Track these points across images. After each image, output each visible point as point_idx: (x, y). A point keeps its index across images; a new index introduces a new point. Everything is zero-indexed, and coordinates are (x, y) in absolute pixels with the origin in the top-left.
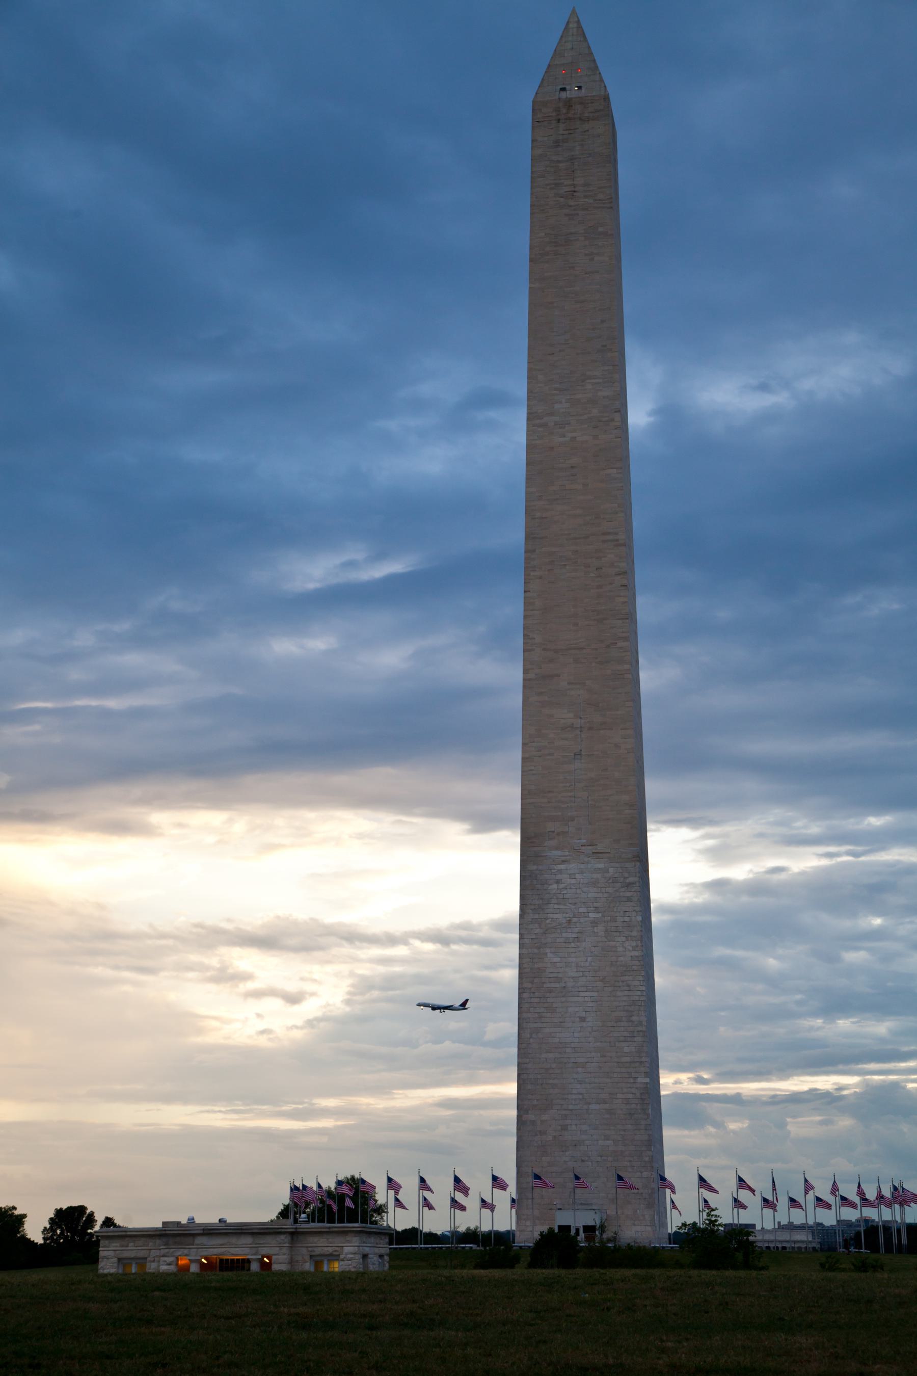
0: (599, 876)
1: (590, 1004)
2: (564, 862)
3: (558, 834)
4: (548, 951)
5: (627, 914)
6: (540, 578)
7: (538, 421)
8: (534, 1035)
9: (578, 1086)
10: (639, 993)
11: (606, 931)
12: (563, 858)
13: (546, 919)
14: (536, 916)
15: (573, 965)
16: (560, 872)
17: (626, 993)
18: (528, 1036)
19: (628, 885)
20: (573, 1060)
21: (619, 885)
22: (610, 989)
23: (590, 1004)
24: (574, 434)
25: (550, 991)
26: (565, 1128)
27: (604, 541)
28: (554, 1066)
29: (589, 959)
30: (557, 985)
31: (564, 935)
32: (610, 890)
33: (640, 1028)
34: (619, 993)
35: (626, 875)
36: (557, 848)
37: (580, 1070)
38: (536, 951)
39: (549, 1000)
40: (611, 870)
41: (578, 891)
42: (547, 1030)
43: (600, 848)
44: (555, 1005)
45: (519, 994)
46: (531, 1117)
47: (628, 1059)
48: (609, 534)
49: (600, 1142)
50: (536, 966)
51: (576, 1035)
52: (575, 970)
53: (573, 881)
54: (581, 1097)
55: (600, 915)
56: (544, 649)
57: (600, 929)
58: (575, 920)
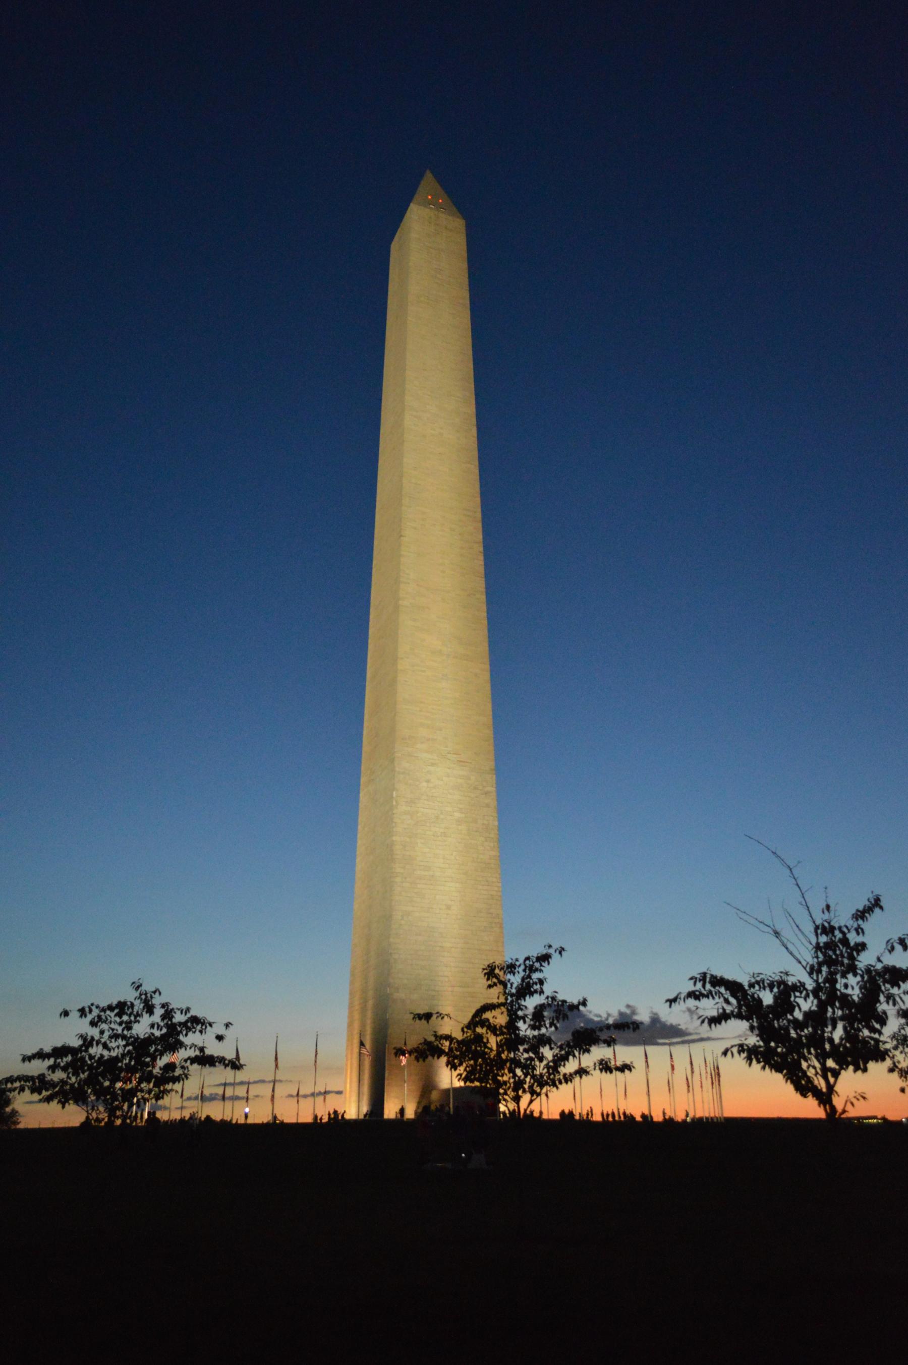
2: (433, 765)
3: (428, 740)
6: (415, 528)
19: (486, 793)
35: (485, 784)
38: (408, 840)
39: (419, 886)
50: (408, 853)
58: (442, 816)
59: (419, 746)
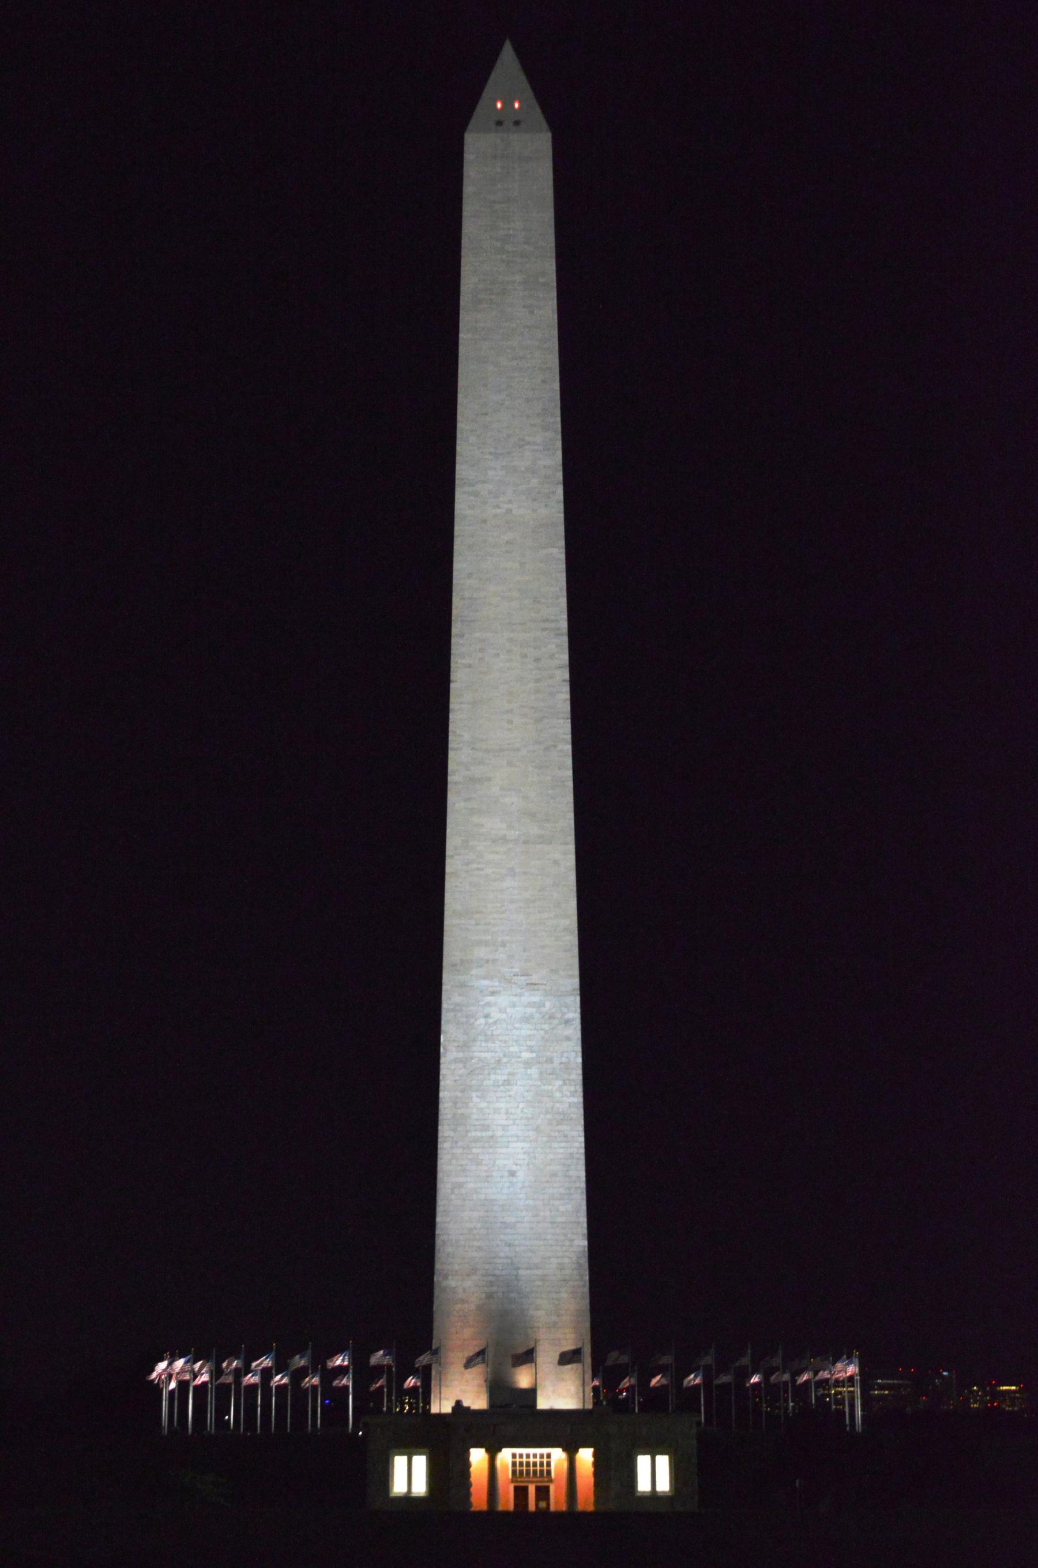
0: (534, 1010)
2: (493, 993)
3: (487, 961)
4: (474, 1095)
5: (565, 1055)
6: (470, 666)
7: (470, 489)
8: (456, 1191)
9: (507, 1249)
10: (577, 1145)
11: (541, 1073)
12: (491, 989)
13: (472, 1058)
14: (461, 1055)
15: (503, 1111)
16: (488, 1004)
17: (563, 1145)
18: (449, 1191)
19: (567, 1022)
20: (501, 1220)
21: (555, 1022)
22: (545, 1139)
23: (522, 1156)
24: (510, 506)
25: (476, 1140)
27: (544, 629)
28: (479, 1225)
29: (521, 1105)
30: (484, 1134)
31: (493, 1077)
32: (546, 1027)
33: (578, 1185)
34: (556, 1145)
35: (565, 1010)
36: (484, 978)
37: (508, 1231)
38: (459, 1094)
39: (474, 1150)
40: (548, 1004)
41: (509, 1027)
42: (472, 1185)
43: (535, 978)
44: (480, 1157)
48: (547, 620)
50: (459, 1111)
51: (505, 1191)
52: (504, 1117)
53: (504, 1016)
55: (534, 1055)
56: (473, 749)
57: (534, 1071)
58: (505, 1060)
59: (474, 972)
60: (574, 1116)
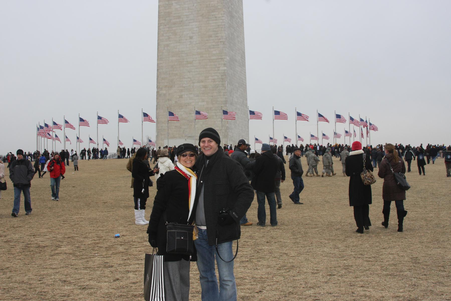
1: (195, 29)
8: (166, 48)
17: (215, 22)
25: (174, 24)
26: (181, 97)
30: (178, 20)
33: (221, 40)
37: (189, 65)
39: (174, 29)
45: (158, 27)
46: (164, 92)
47: (214, 58)
49: (200, 103)
50: (167, 11)
54: (189, 79)
60: (220, 7)
